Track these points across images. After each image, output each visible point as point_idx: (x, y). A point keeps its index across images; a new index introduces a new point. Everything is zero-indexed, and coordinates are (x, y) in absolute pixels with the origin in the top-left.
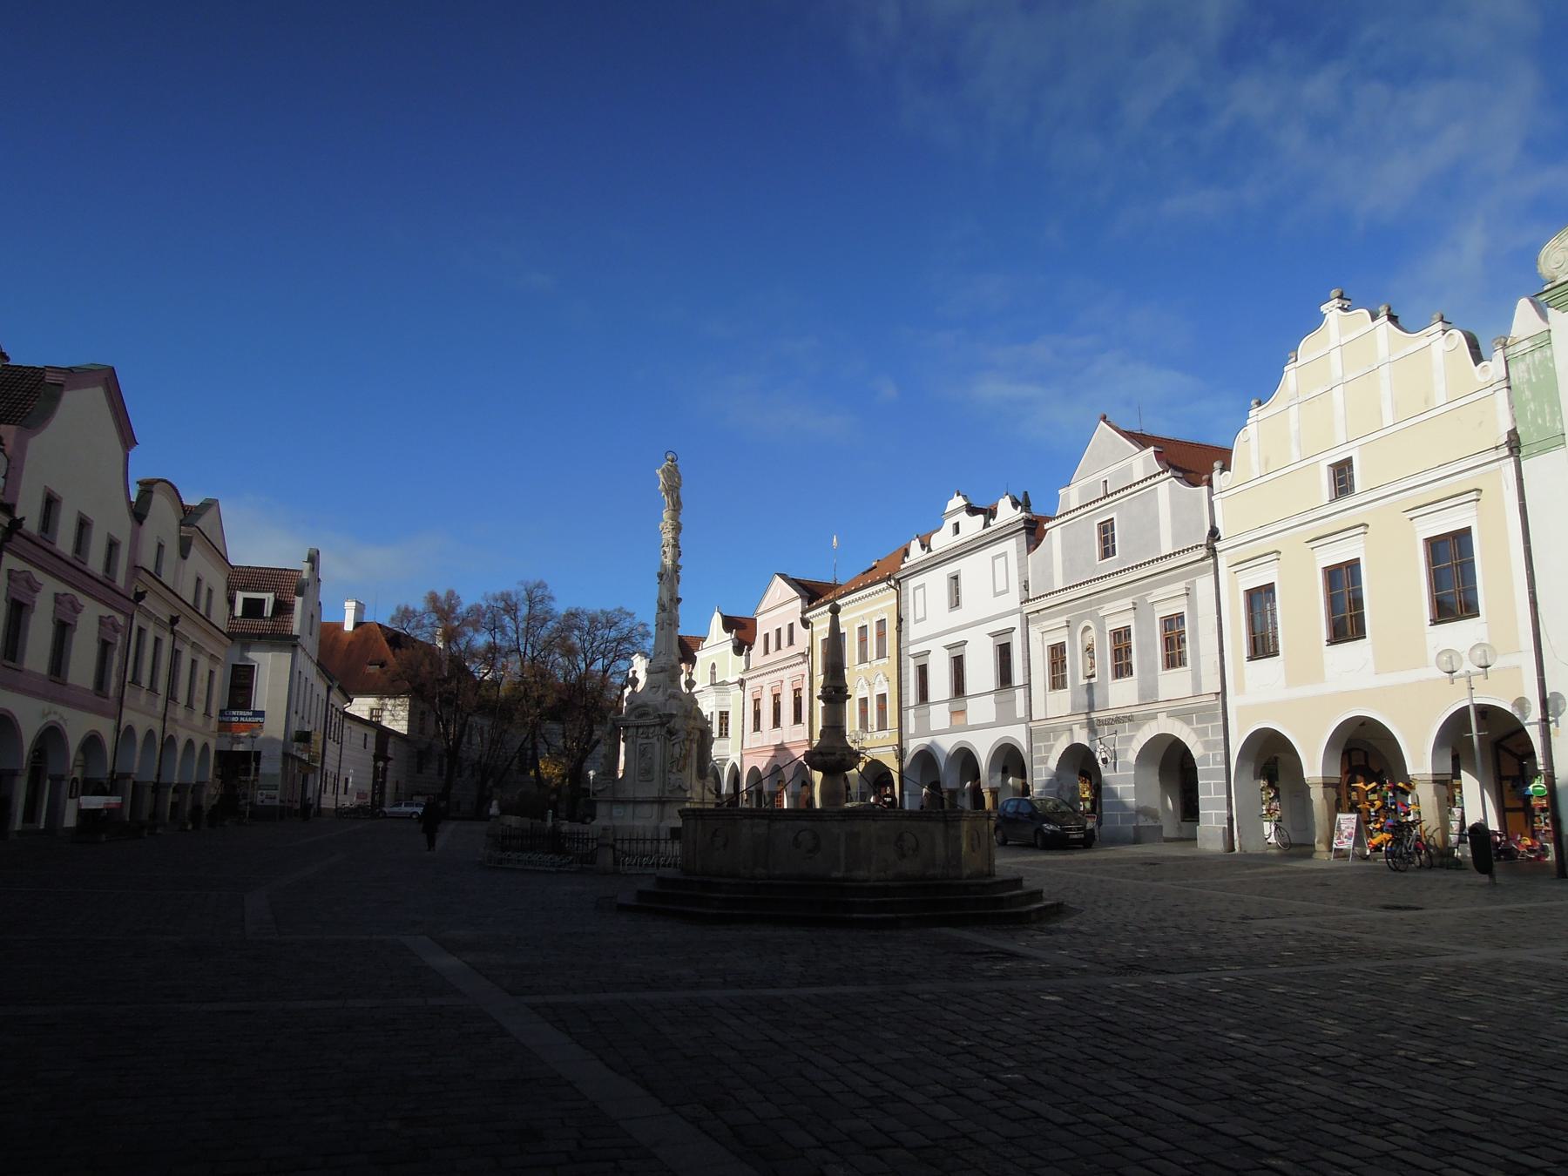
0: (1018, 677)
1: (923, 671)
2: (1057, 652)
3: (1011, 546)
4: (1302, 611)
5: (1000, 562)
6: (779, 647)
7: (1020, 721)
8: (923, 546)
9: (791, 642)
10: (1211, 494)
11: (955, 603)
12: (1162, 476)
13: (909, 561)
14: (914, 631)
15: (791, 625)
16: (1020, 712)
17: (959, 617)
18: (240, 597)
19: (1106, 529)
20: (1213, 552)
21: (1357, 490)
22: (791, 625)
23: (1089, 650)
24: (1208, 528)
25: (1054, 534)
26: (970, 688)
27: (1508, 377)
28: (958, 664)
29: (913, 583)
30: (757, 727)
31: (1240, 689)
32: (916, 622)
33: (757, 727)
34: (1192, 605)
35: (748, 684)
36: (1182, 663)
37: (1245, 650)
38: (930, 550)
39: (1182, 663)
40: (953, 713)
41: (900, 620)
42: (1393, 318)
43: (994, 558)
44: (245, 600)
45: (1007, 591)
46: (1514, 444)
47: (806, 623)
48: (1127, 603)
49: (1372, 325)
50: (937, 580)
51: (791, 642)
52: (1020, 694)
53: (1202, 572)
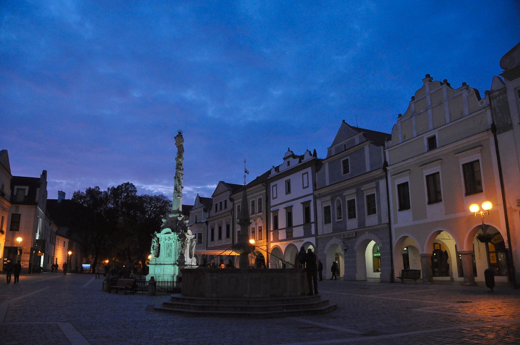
0: (312, 220)
2: (327, 210)
3: (309, 170)
4: (418, 193)
5: (305, 176)
6: (221, 209)
7: (312, 236)
8: (276, 171)
9: (226, 207)
10: (384, 149)
11: (288, 191)
12: (366, 143)
13: (271, 176)
14: (273, 202)
15: (226, 201)
16: (313, 232)
17: (289, 197)
18: (16, 187)
19: (346, 162)
20: (385, 170)
21: (438, 147)
22: (226, 201)
23: (339, 208)
24: (383, 162)
25: (326, 167)
26: (294, 225)
27: (490, 104)
29: (272, 184)
30: (212, 239)
31: (396, 222)
32: (273, 199)
33: (212, 239)
35: (209, 223)
36: (374, 212)
37: (398, 208)
38: (278, 172)
40: (287, 233)
43: (303, 174)
44: (18, 189)
45: (308, 187)
46: (494, 129)
47: (232, 200)
48: (354, 190)
49: (441, 87)
50: (281, 184)
51: (226, 207)
52: (313, 225)
53: (381, 178)
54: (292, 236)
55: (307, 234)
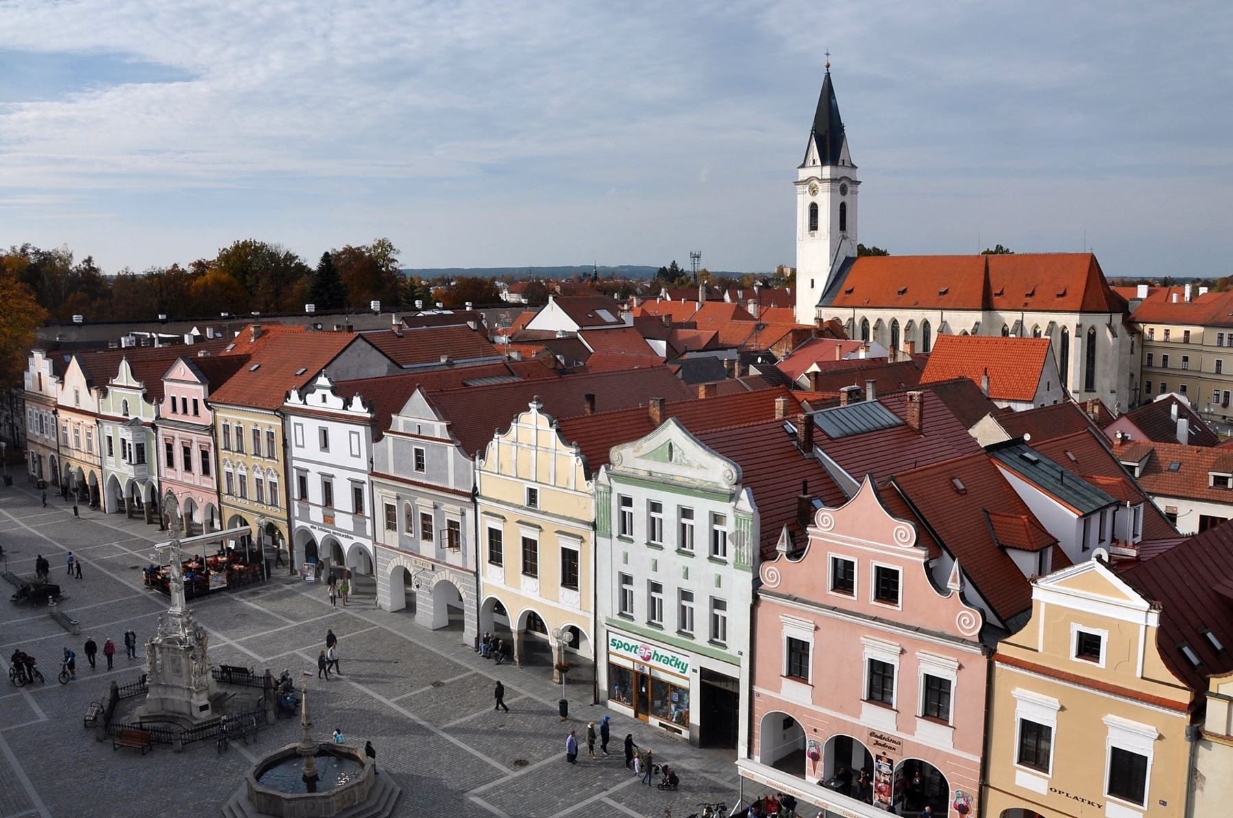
1: (303, 481)
5: (354, 437)
7: (368, 537)
14: (295, 452)
28: (327, 488)
34: (464, 521)
39: (458, 546)
41: (285, 440)
42: (557, 430)
43: (351, 432)
52: (368, 522)
54: (333, 522)
55: (359, 530)
